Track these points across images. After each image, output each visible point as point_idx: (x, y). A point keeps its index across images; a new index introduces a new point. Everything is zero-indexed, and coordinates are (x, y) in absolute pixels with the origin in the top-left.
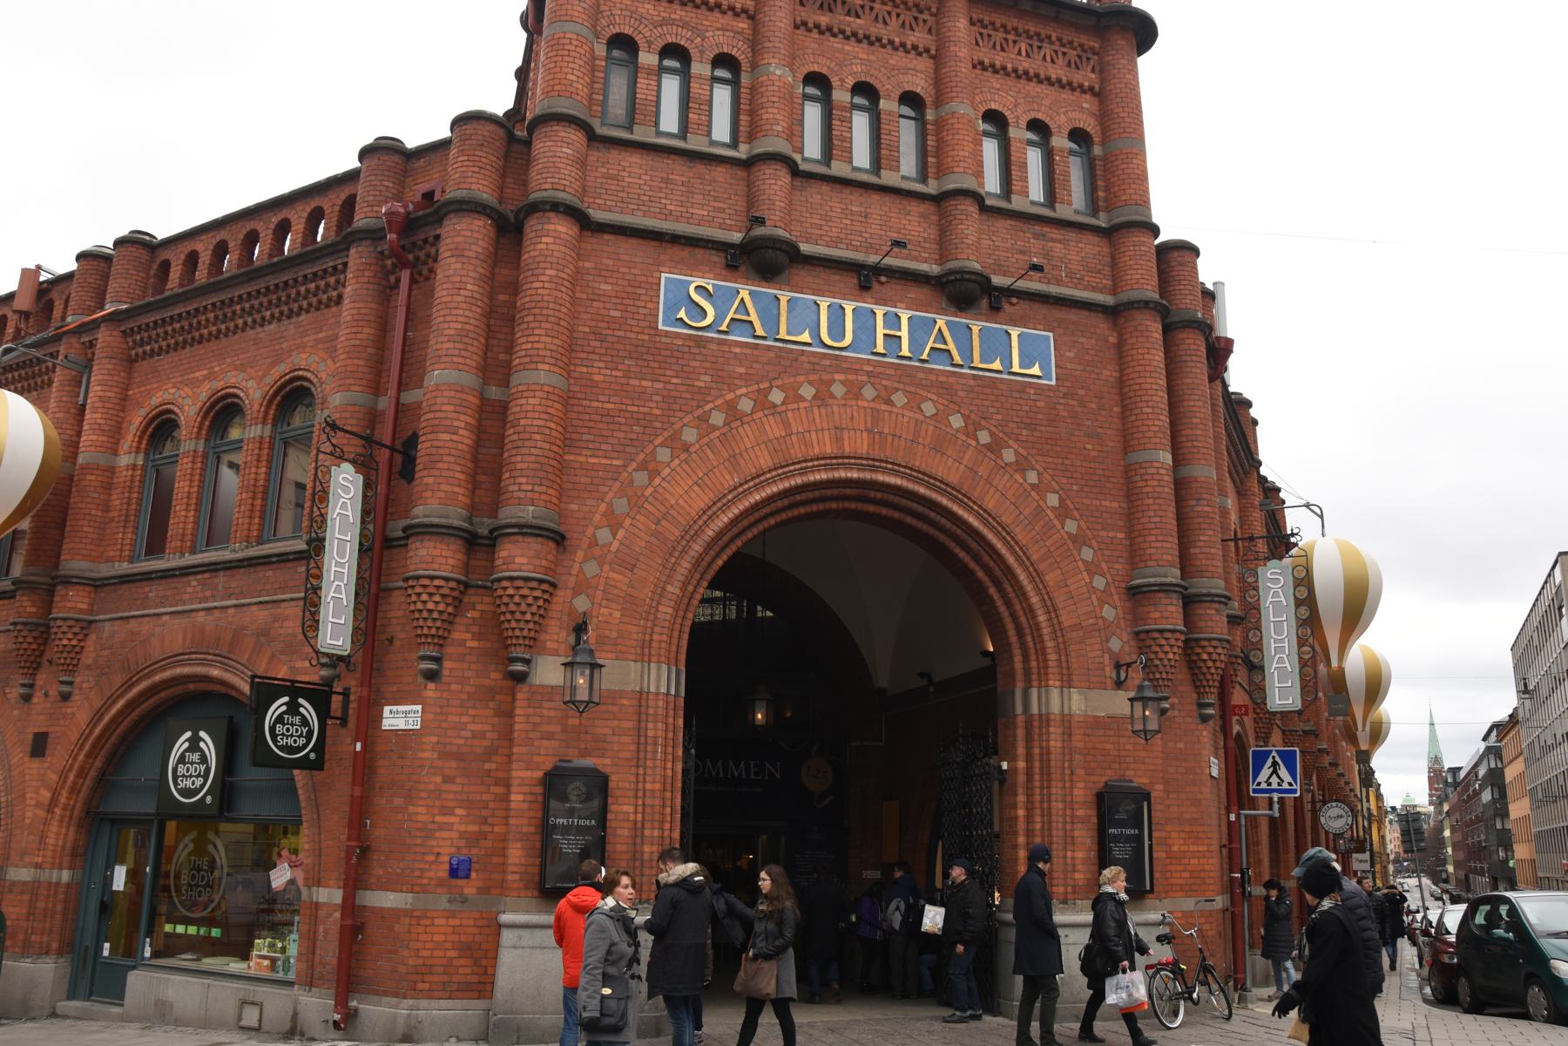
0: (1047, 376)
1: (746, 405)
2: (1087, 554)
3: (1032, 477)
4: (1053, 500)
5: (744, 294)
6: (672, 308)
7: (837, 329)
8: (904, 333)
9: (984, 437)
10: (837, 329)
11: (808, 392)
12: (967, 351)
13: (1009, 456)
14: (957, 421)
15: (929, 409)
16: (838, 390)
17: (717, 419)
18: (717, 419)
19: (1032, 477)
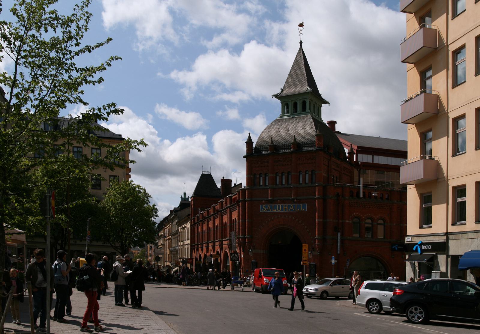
0: (305, 210)
1: (269, 220)
2: (310, 234)
3: (303, 224)
4: (306, 227)
5: (269, 206)
6: (261, 209)
7: (279, 209)
8: (287, 208)
9: (297, 220)
10: (279, 209)
11: (276, 217)
12: (295, 209)
13: (300, 222)
14: (294, 218)
15: (290, 217)
16: (279, 216)
17: (267, 222)
18: (267, 222)
19: (303, 224)
